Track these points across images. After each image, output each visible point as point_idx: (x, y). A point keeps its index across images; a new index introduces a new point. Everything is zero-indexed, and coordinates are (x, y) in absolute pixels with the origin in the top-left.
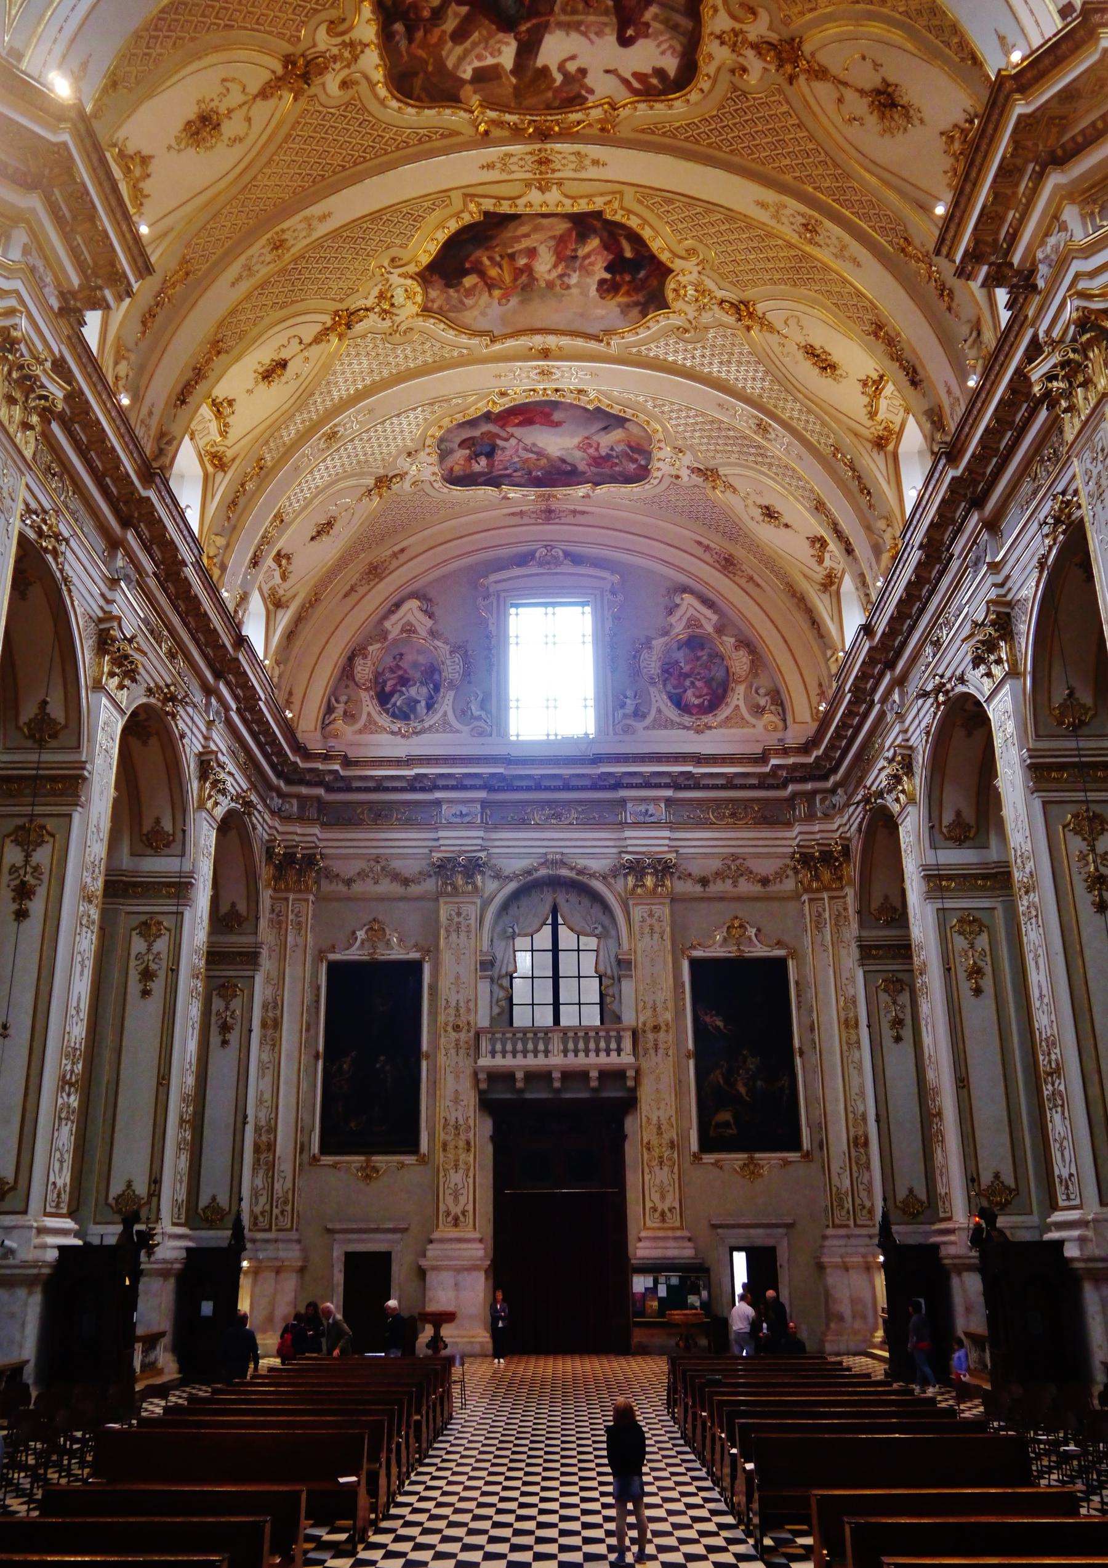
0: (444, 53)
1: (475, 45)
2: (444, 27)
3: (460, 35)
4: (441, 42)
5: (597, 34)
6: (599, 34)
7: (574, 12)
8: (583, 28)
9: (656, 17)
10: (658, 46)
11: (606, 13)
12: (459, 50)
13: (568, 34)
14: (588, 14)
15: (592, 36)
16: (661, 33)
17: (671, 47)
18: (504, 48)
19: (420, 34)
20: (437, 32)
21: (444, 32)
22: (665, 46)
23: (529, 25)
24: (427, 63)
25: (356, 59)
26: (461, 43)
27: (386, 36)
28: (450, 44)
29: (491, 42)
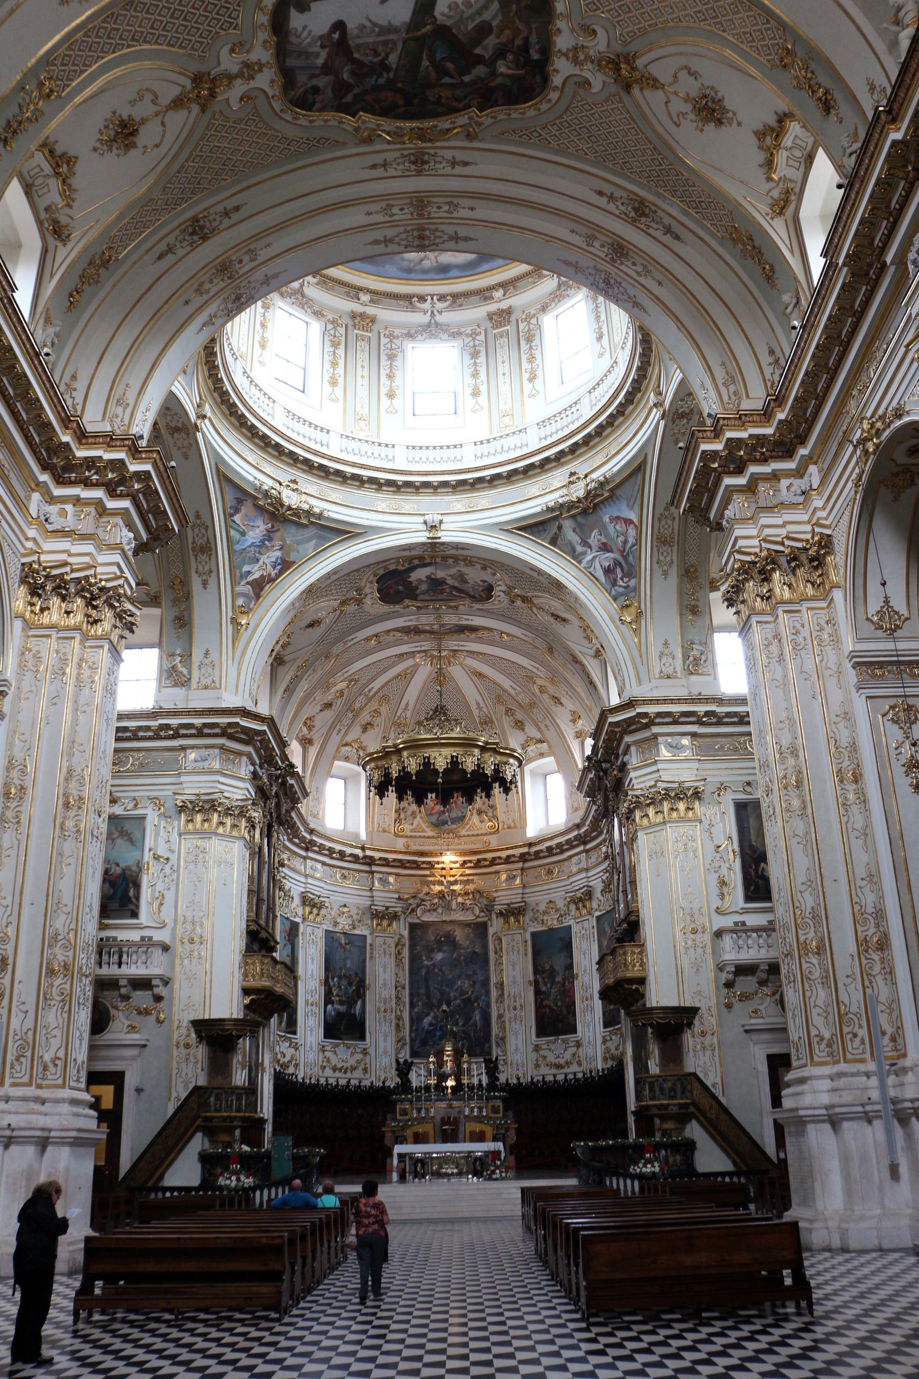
0: (500, 17)
1: (472, 18)
2: (497, 41)
3: (484, 30)
4: (501, 29)
5: (364, 27)
6: (362, 27)
7: (385, 43)
8: (377, 30)
9: (317, 55)
10: (310, 32)
11: (359, 47)
12: (486, 16)
13: (390, 23)
14: (374, 43)
15: (368, 24)
16: (309, 44)
17: (300, 36)
18: (446, 11)
19: (518, 42)
20: (503, 39)
21: (498, 37)
22: (304, 35)
23: (424, 30)
24: (516, 13)
25: (575, 49)
26: (484, 22)
27: (546, 51)
28: (494, 24)
29: (457, 18)
